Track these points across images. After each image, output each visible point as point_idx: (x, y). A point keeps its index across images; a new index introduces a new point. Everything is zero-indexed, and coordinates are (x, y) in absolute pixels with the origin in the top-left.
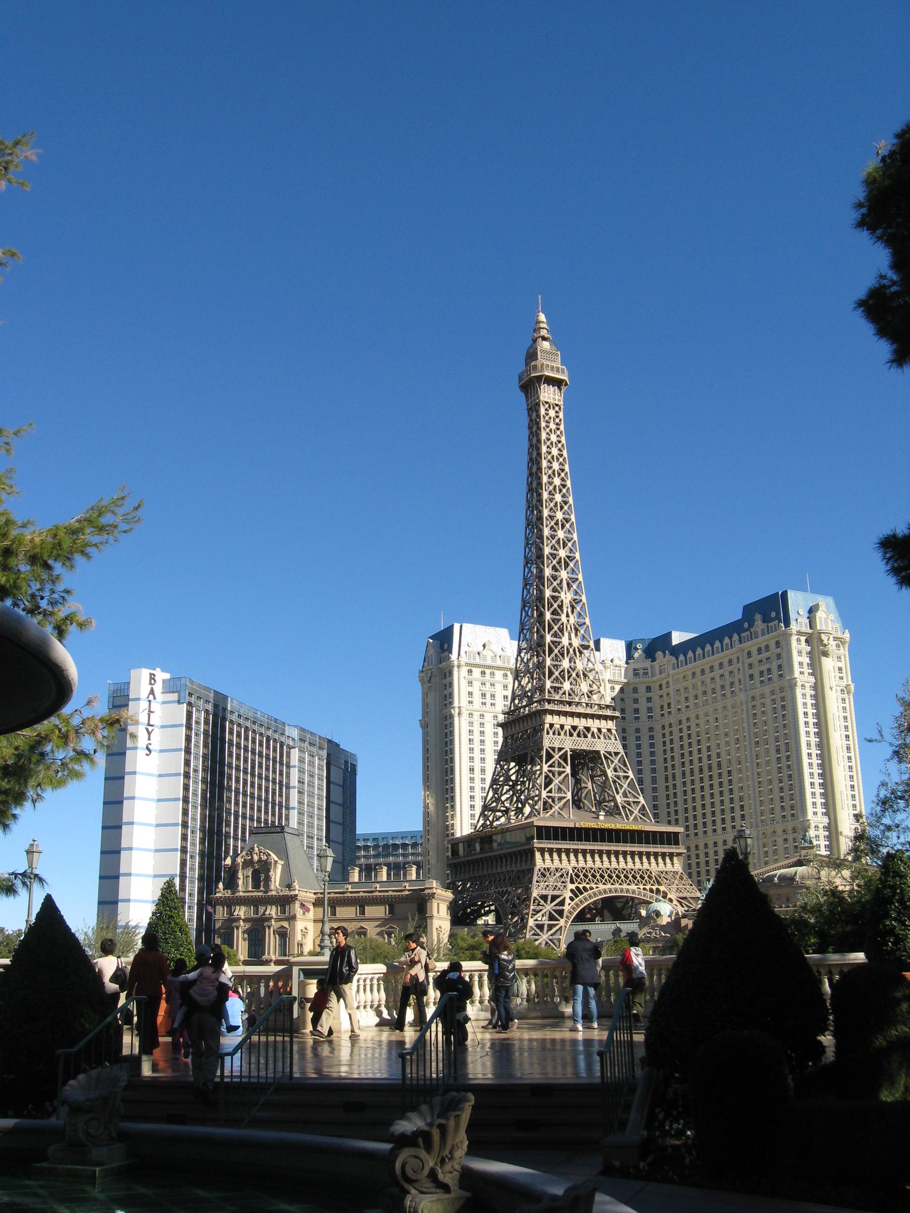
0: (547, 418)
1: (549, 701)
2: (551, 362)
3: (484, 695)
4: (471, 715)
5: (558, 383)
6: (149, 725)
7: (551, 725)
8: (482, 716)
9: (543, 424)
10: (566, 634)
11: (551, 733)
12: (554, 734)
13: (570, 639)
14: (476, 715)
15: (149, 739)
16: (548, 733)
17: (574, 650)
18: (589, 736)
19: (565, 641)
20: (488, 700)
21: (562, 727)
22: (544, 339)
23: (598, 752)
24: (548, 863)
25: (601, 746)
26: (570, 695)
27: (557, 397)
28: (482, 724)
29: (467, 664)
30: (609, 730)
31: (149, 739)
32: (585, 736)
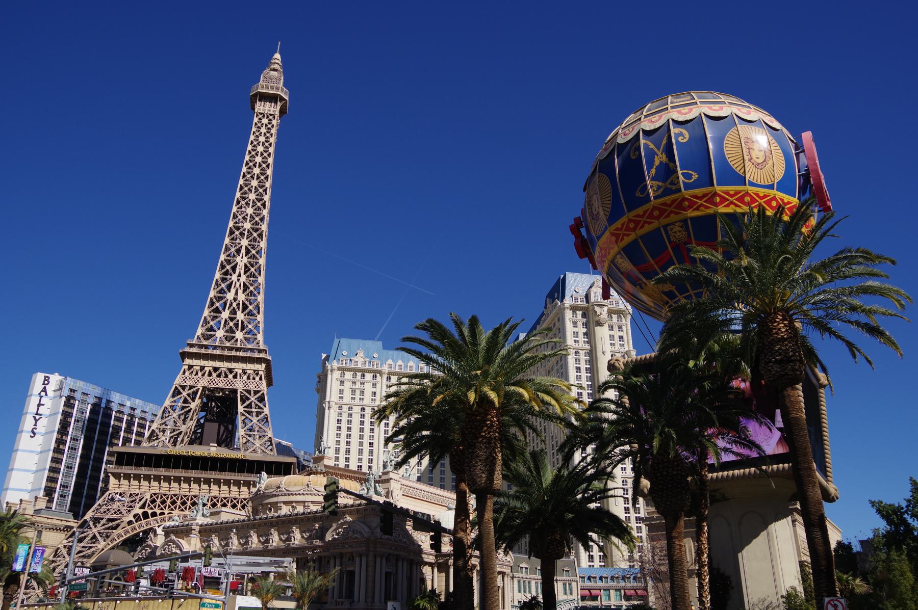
3: (353, 392)
4: (340, 408)
5: (273, 98)
6: (37, 414)
7: (191, 367)
8: (351, 408)
10: (233, 290)
13: (236, 294)
14: (345, 408)
15: (35, 425)
17: (238, 304)
18: (230, 376)
19: (230, 296)
20: (358, 396)
22: (275, 70)
23: (236, 390)
26: (221, 340)
27: (272, 109)
28: (350, 415)
29: (339, 369)
30: (256, 372)
31: (35, 425)
32: (226, 376)
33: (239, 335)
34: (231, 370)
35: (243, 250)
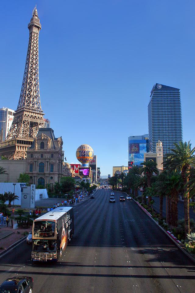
0: (34, 36)
1: (26, 108)
2: (37, 23)
5: (38, 27)
7: (26, 115)
9: (33, 38)
11: (25, 116)
12: (26, 117)
13: (33, 93)
16: (24, 116)
18: (36, 118)
19: (32, 94)
21: (29, 115)
22: (36, 16)
24: (19, 150)
25: (39, 121)
30: (41, 118)
32: (35, 118)
33: (36, 106)
34: (36, 117)
35: (34, 79)
